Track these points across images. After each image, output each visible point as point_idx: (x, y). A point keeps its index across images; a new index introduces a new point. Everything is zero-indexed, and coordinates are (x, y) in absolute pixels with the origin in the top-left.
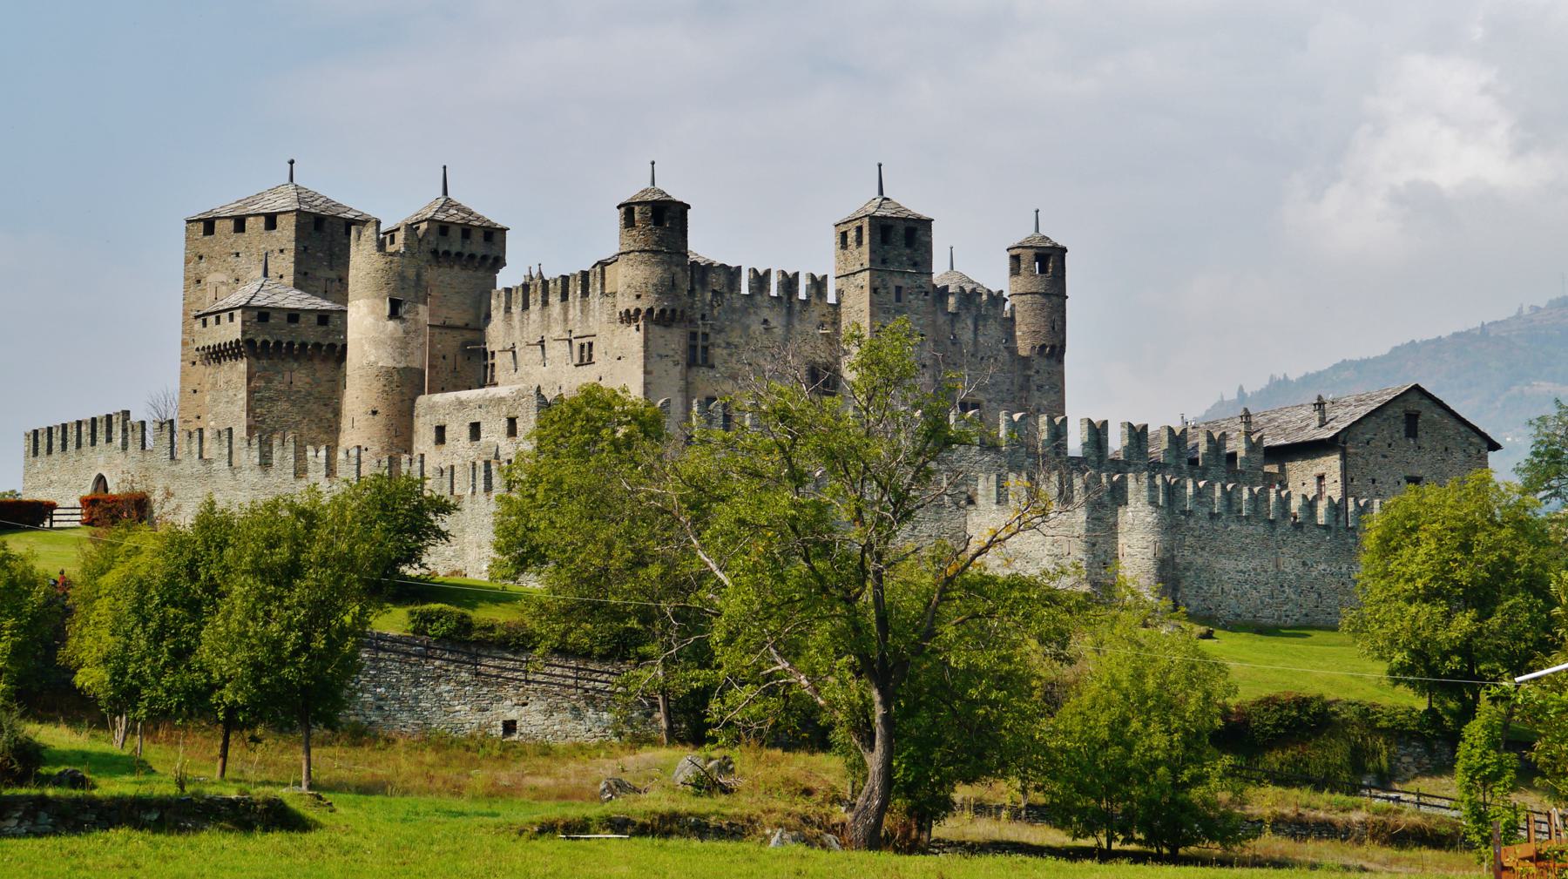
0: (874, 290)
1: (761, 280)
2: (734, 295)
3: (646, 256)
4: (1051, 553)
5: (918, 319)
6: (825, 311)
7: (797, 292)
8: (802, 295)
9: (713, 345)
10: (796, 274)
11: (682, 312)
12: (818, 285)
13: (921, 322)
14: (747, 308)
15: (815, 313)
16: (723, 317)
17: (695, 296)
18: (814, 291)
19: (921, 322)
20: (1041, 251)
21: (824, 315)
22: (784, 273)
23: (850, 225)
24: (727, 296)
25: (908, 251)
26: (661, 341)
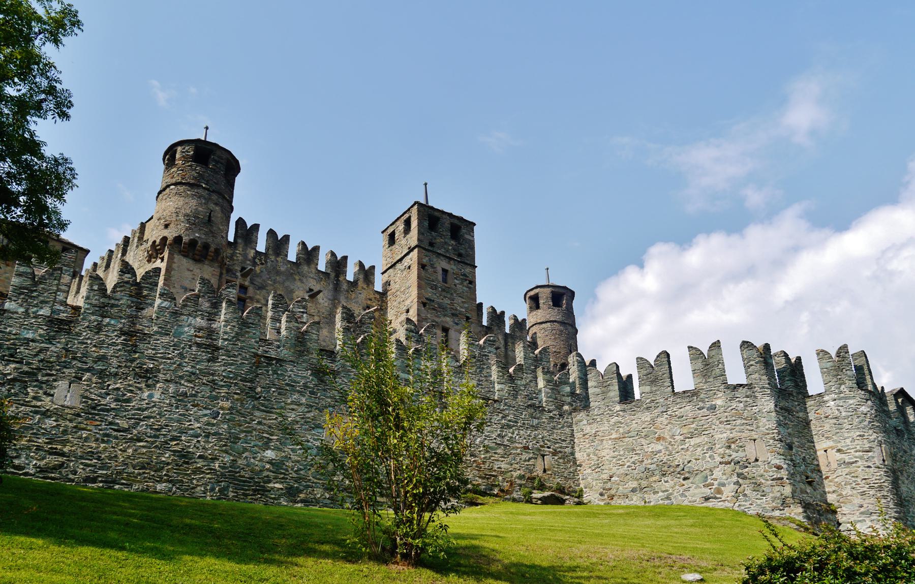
0: (422, 266)
1: (309, 255)
2: (279, 259)
3: (181, 188)
4: (727, 459)
5: (463, 302)
6: (372, 296)
7: (345, 273)
8: (350, 277)
9: (251, 299)
10: (345, 258)
11: (217, 251)
12: (367, 274)
13: (466, 305)
14: (292, 274)
15: (362, 295)
16: (265, 276)
17: (236, 248)
18: (361, 277)
19: (466, 305)
20: (557, 290)
21: (370, 300)
22: (333, 254)
23: (398, 223)
24: (273, 258)
25: (453, 242)
26: (188, 273)
